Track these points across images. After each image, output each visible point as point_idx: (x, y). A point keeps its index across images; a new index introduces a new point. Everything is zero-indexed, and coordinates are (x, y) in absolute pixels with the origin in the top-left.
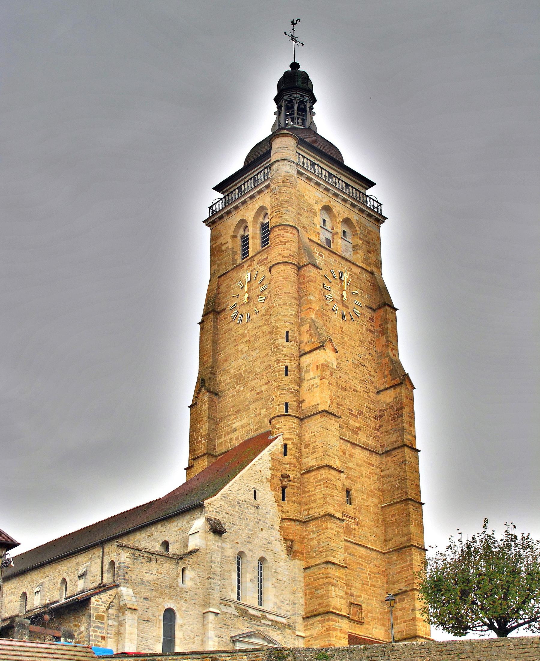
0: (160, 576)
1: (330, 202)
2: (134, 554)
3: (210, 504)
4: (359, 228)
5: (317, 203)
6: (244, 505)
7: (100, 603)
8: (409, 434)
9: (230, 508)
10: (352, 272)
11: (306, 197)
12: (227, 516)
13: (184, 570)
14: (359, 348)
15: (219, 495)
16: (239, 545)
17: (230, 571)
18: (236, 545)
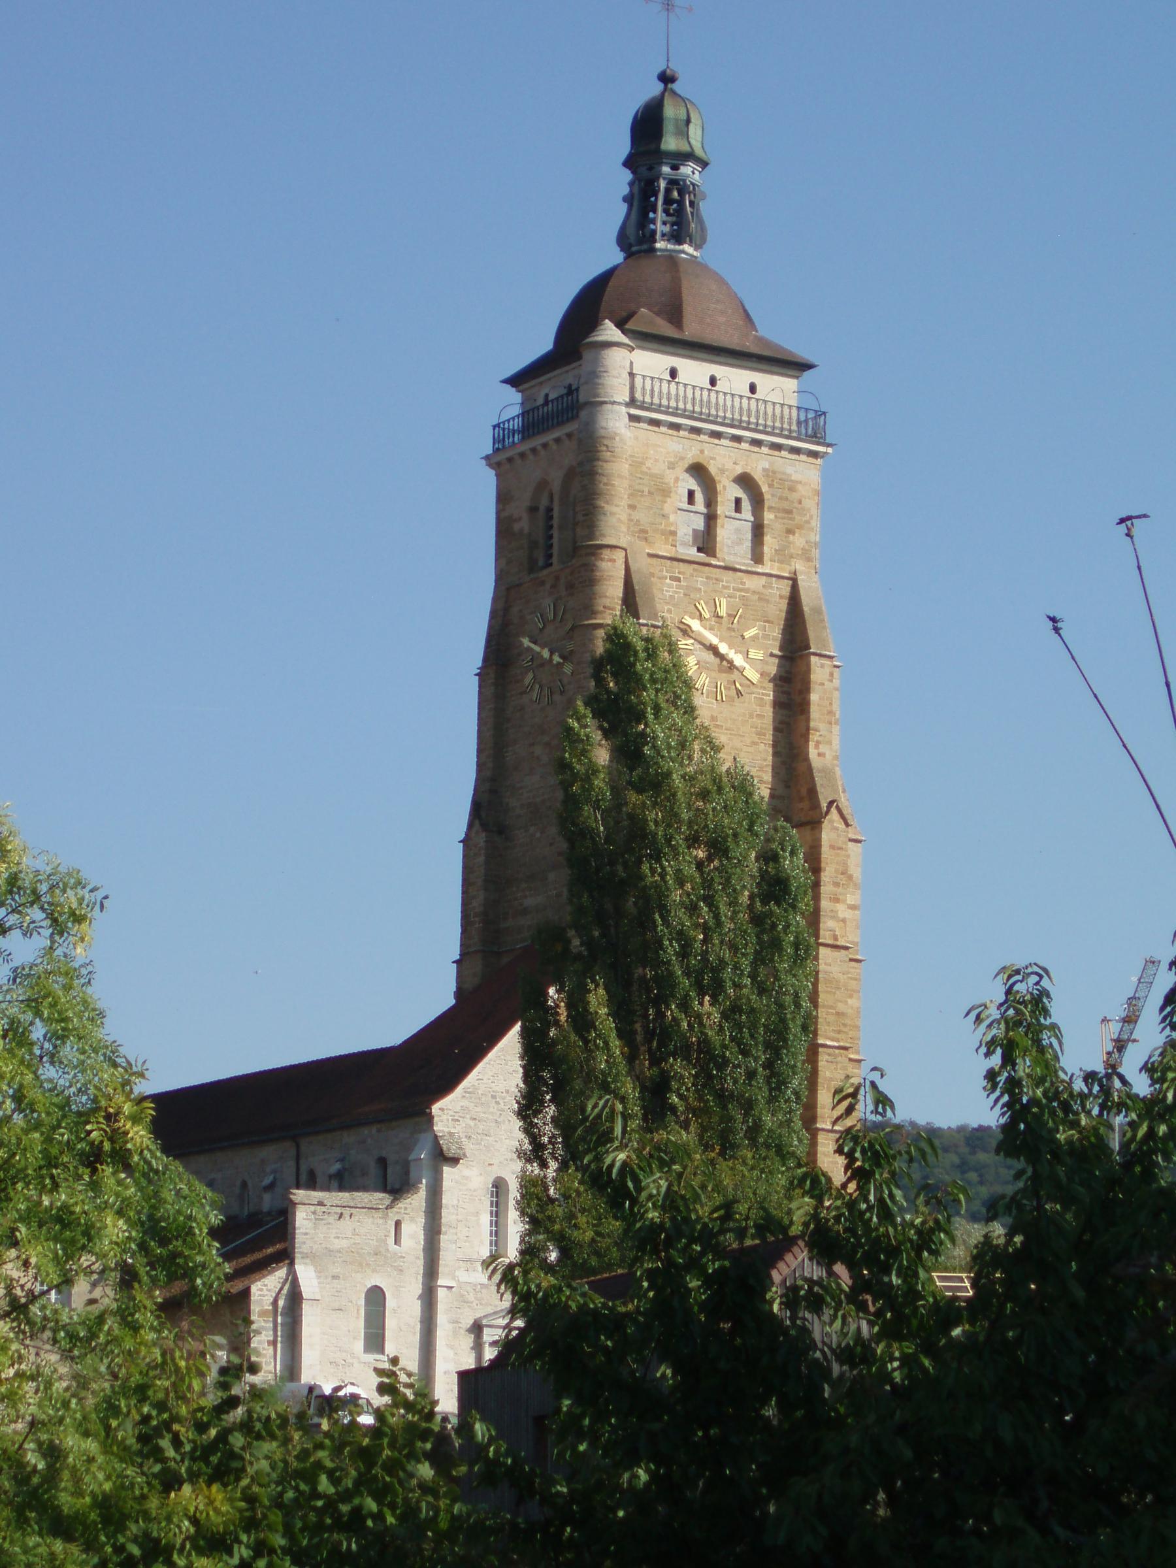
0: (358, 1240)
1: (702, 452)
2: (314, 1213)
3: (442, 1109)
4: (770, 486)
5: (671, 466)
6: (504, 1098)
7: (265, 1292)
8: (833, 918)
9: (479, 1109)
10: (747, 590)
11: (649, 464)
12: (472, 1123)
13: (398, 1224)
14: (751, 749)
15: (459, 1090)
16: (494, 1168)
17: (477, 1214)
18: (490, 1168)
